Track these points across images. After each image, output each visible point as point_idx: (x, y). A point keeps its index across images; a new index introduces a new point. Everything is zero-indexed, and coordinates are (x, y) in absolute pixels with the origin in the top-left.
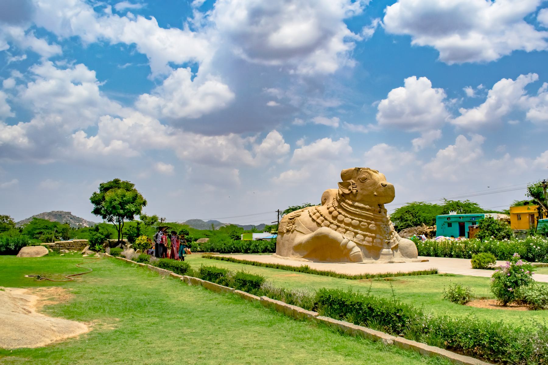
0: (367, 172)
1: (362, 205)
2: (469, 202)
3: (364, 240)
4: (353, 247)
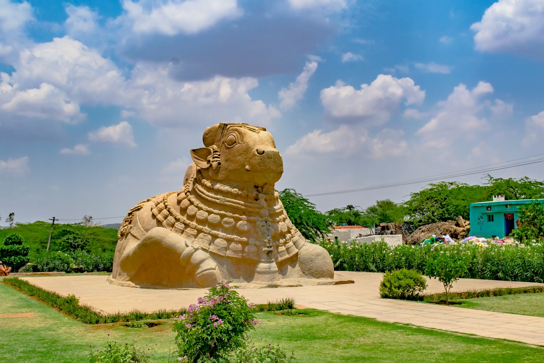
0: (236, 130)
1: (226, 188)
2: (530, 180)
3: (226, 249)
4: (202, 261)
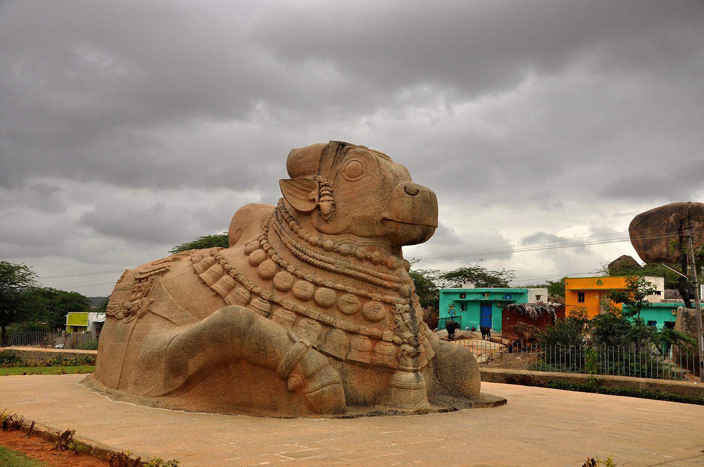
4: (319, 370)
